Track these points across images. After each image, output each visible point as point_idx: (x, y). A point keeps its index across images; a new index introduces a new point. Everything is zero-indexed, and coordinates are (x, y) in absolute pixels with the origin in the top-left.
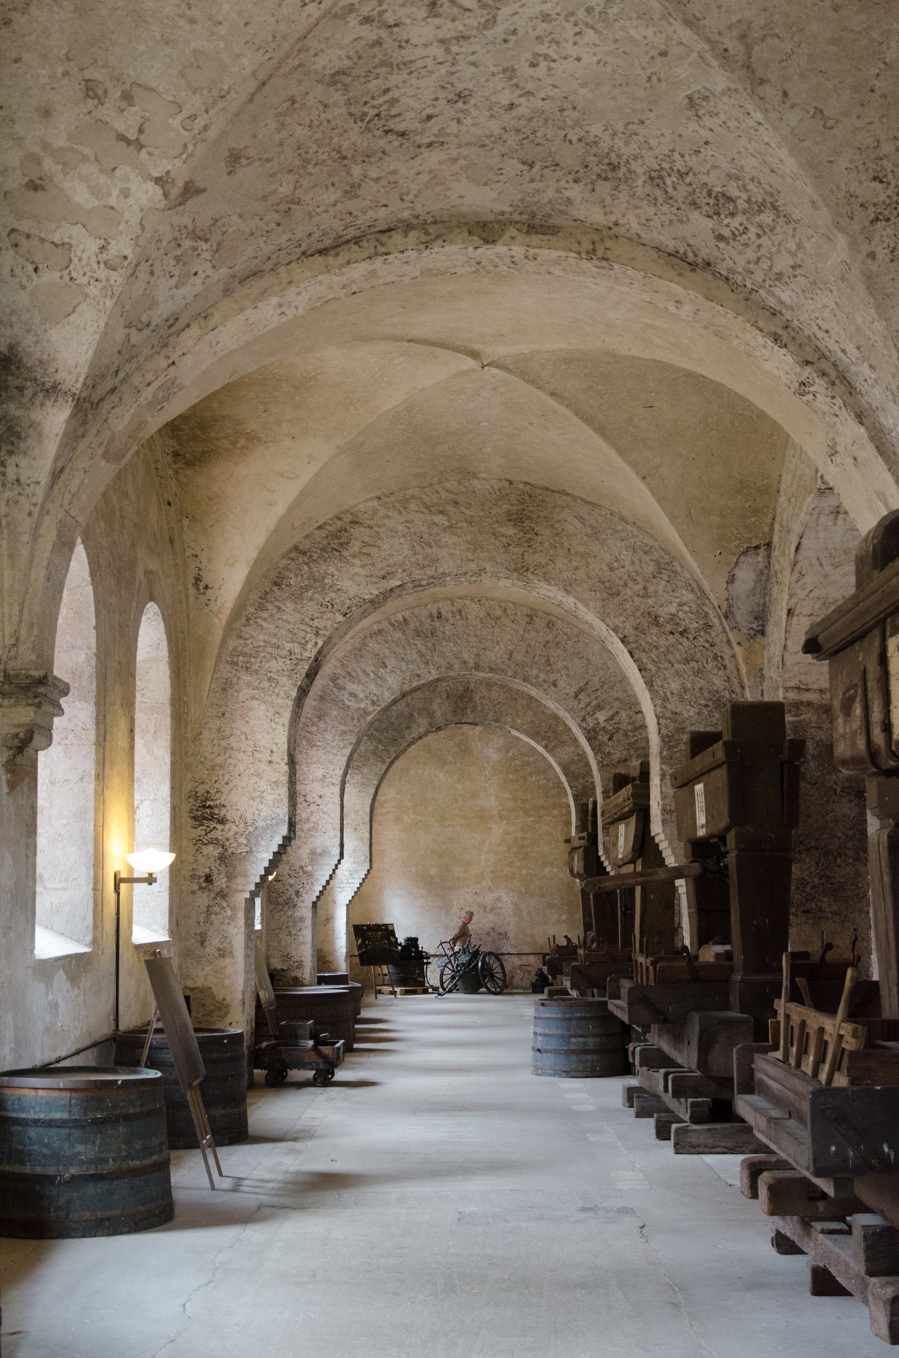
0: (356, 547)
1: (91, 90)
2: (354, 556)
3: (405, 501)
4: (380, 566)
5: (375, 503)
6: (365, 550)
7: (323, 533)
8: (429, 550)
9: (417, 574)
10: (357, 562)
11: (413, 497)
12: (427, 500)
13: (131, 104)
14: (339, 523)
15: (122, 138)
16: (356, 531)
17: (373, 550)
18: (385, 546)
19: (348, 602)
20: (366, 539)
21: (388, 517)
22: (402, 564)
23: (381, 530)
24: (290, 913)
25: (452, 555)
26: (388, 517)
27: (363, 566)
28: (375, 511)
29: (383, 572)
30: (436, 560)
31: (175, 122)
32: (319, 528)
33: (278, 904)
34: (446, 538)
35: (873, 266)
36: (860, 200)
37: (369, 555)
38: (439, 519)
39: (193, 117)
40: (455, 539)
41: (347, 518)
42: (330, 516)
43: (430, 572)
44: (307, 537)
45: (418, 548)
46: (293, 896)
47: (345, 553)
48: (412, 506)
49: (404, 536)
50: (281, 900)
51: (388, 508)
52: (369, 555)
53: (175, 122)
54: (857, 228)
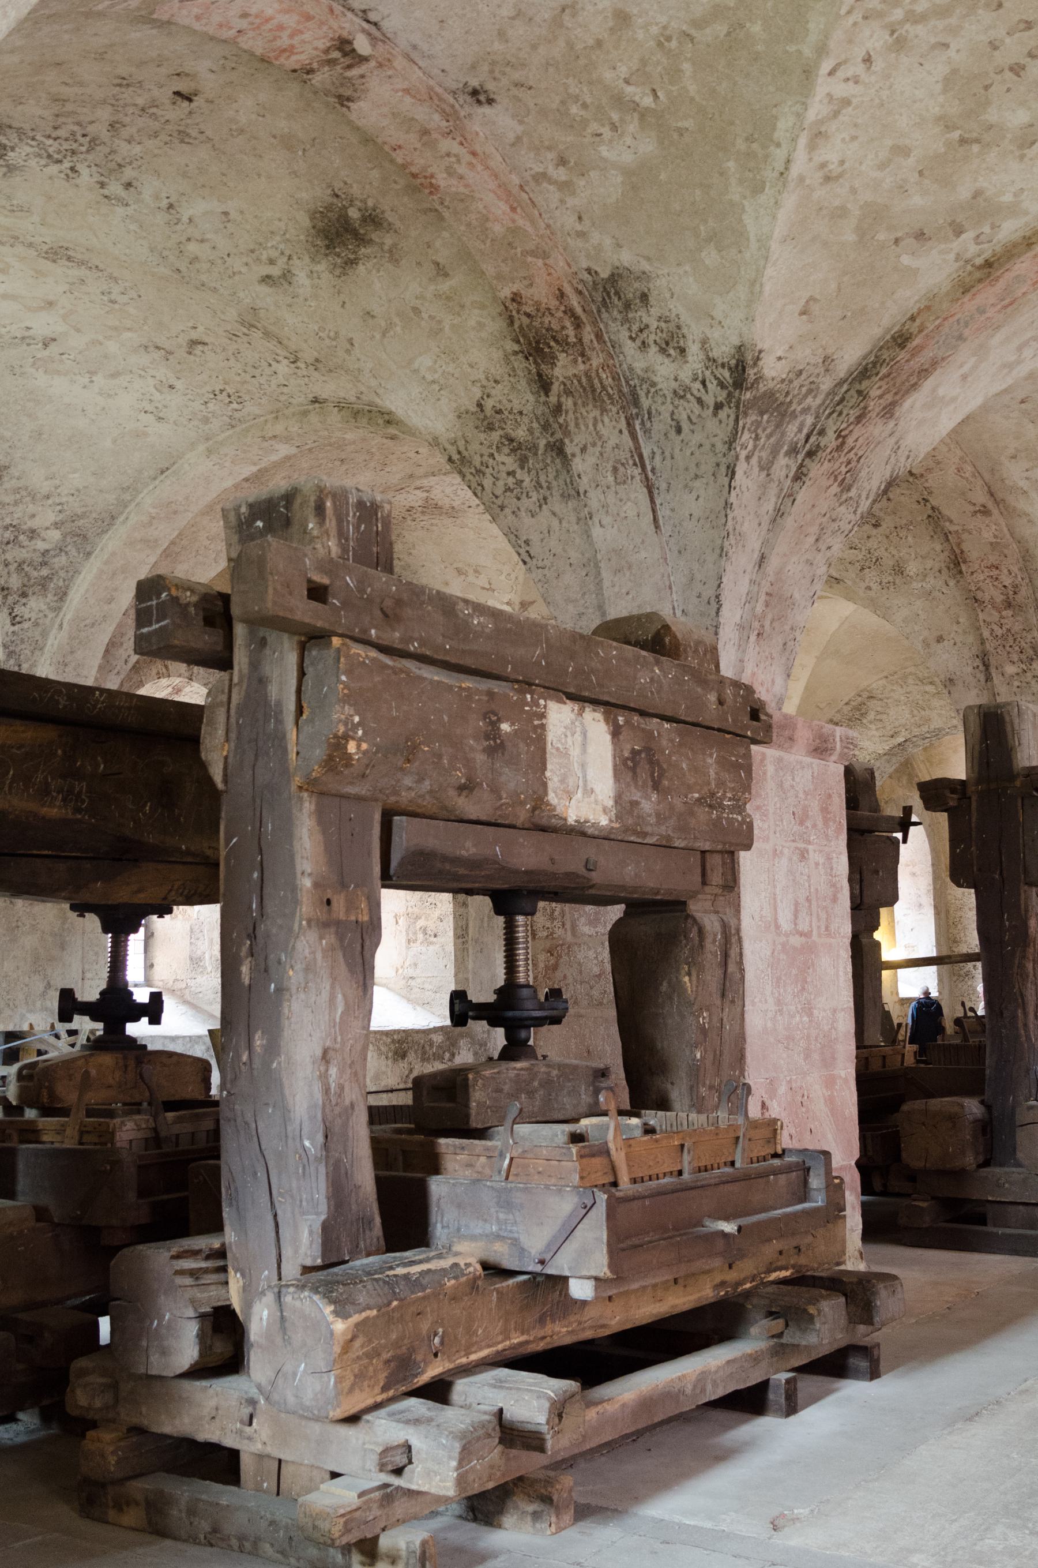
0: (871, 715)
1: (459, 571)
2: (871, 722)
3: (905, 677)
4: (889, 728)
5: (884, 682)
6: (878, 717)
7: (849, 708)
8: (923, 713)
9: (916, 731)
10: (873, 727)
11: (911, 674)
12: (920, 675)
13: (480, 574)
14: (860, 699)
15: (483, 588)
16: (872, 704)
17: (884, 717)
18: (891, 713)
19: (868, 757)
20: (879, 709)
21: (893, 690)
22: (904, 726)
23: (889, 701)
24: (969, 983)
25: (940, 715)
26: (893, 690)
27: (877, 729)
28: (884, 688)
29: (891, 733)
30: (929, 720)
31: (503, 577)
32: (847, 704)
33: (960, 976)
34: (936, 703)
35: (872, 594)
36: (848, 560)
37: (881, 720)
38: (930, 688)
39: (509, 575)
40: (942, 703)
41: (865, 695)
42: (853, 694)
43: (925, 729)
44: (839, 711)
45: (915, 712)
46: (972, 969)
47: (865, 721)
48: (910, 681)
49: (905, 704)
50: (962, 972)
51: (893, 684)
52: (881, 720)
53: (503, 577)
54: (854, 576)
